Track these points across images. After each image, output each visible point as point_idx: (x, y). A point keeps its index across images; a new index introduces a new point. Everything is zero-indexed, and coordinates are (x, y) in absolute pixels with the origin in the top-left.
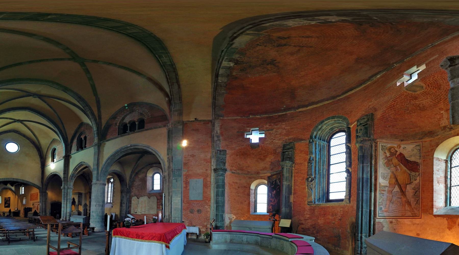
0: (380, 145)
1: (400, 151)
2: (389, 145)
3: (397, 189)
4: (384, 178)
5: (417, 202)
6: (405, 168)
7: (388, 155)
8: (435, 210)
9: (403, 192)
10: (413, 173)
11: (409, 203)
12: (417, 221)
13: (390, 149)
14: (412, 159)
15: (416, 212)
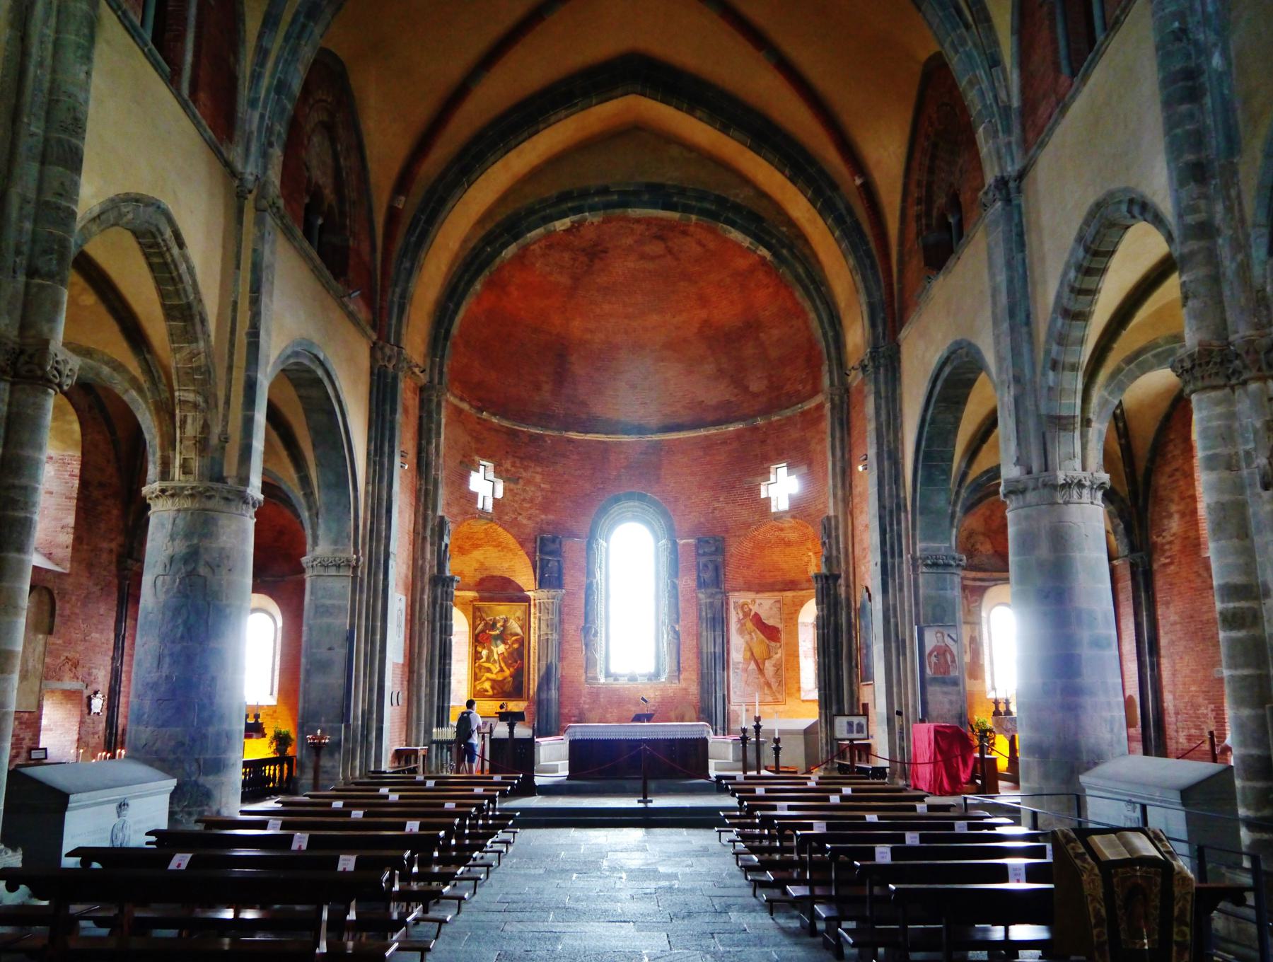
0: (732, 601)
1: (755, 609)
2: (742, 601)
3: (753, 666)
4: (737, 651)
5: (780, 683)
6: (761, 636)
7: (741, 616)
8: (802, 694)
9: (761, 670)
10: (773, 644)
11: (769, 685)
12: (780, 708)
13: (742, 607)
14: (770, 622)
15: (779, 696)
